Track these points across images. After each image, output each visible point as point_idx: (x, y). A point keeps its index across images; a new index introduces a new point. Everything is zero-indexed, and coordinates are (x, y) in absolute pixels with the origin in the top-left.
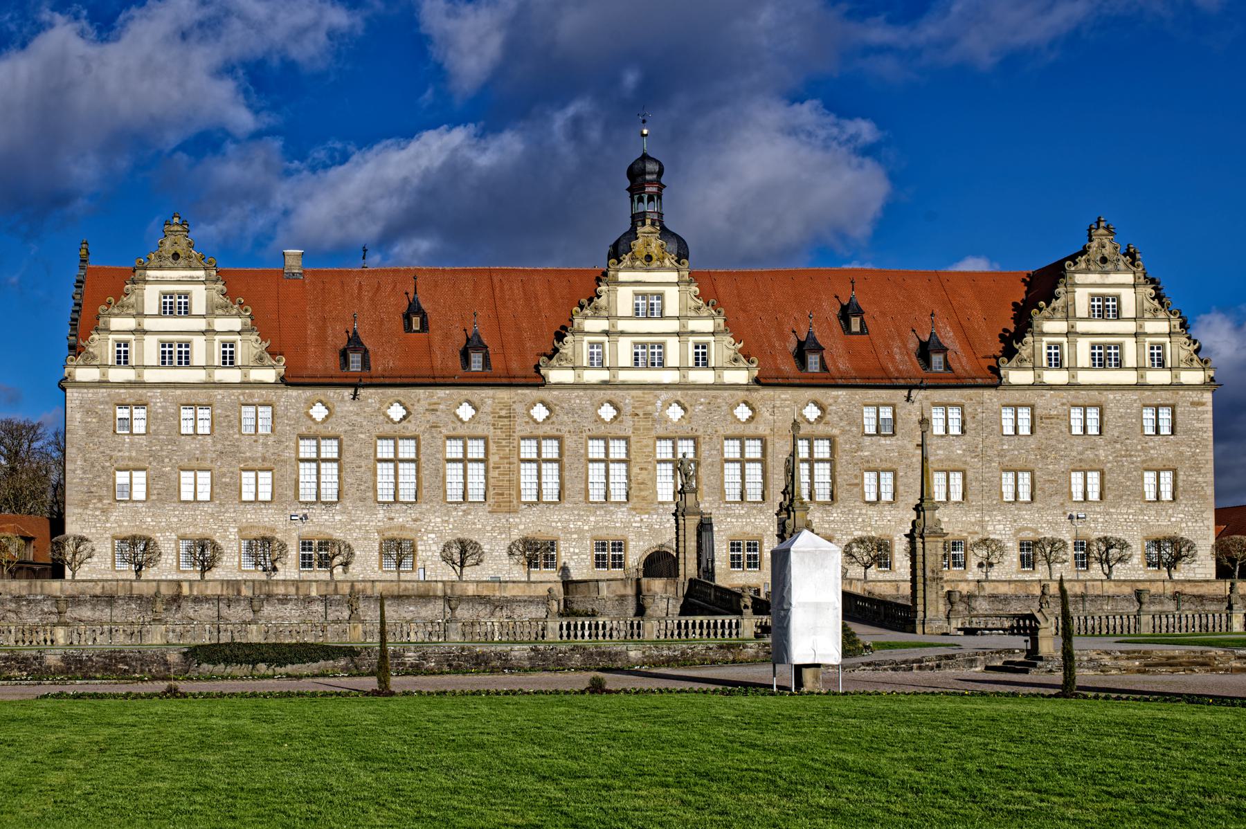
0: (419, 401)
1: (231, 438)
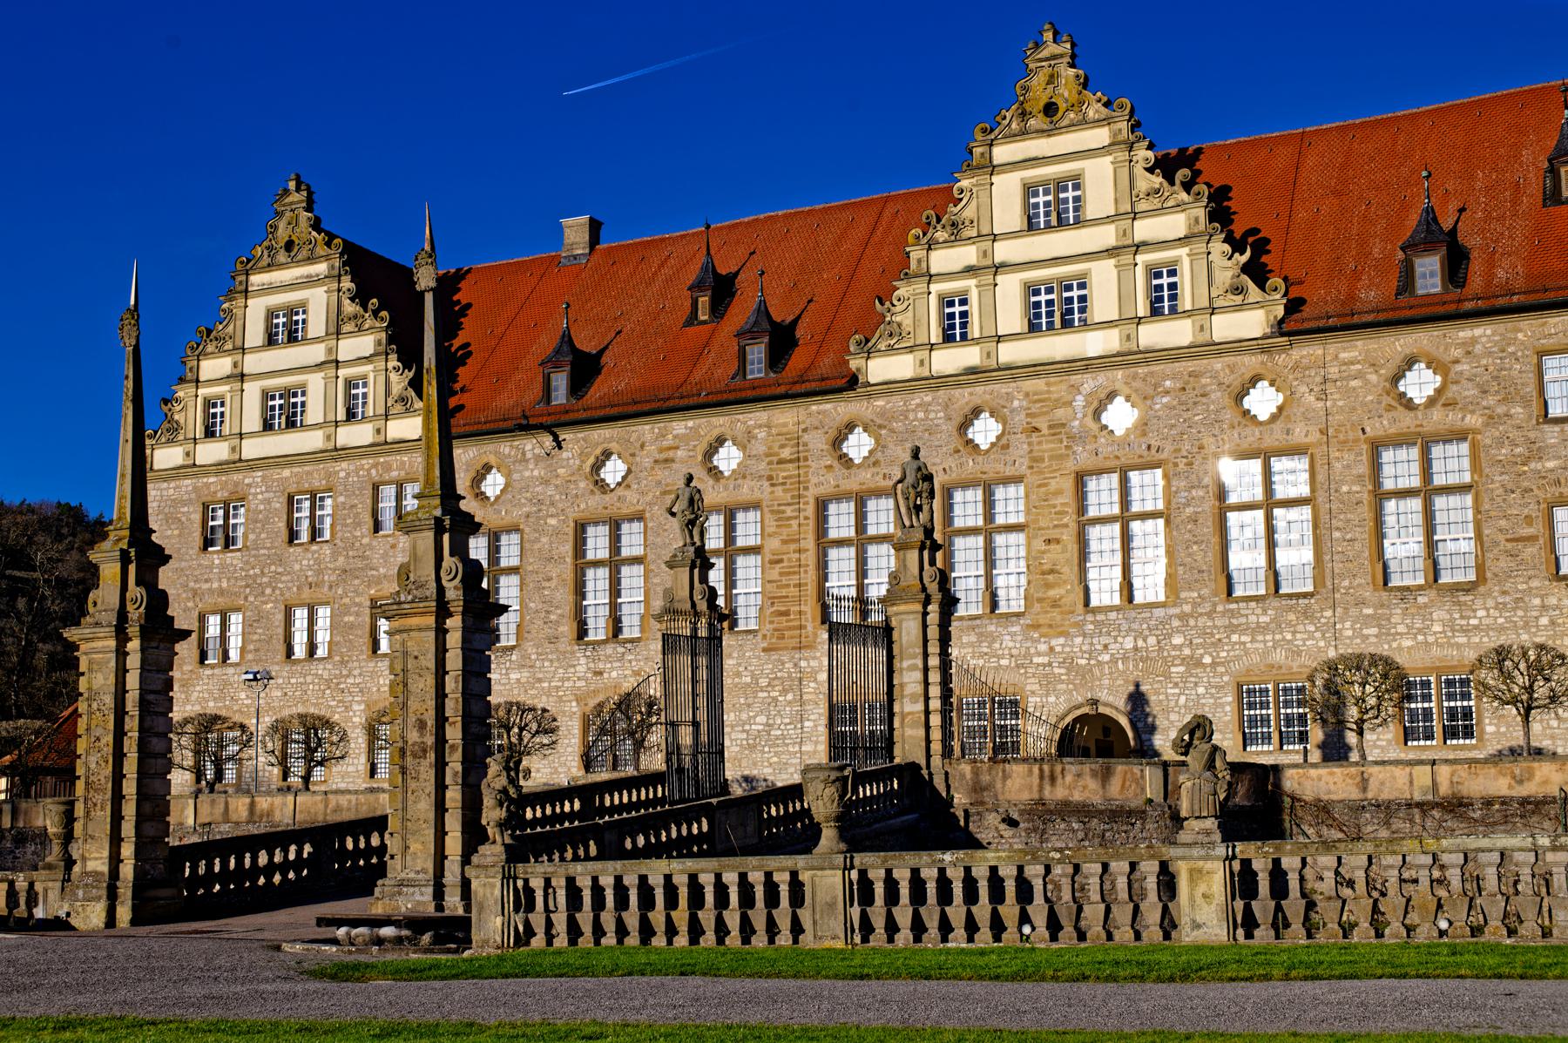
0: (642, 446)
1: (357, 544)
